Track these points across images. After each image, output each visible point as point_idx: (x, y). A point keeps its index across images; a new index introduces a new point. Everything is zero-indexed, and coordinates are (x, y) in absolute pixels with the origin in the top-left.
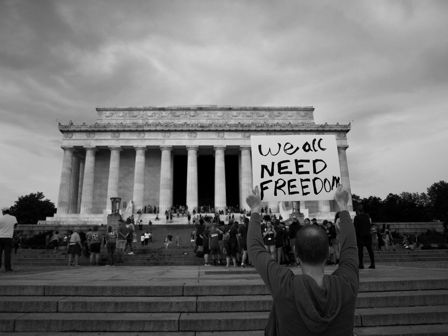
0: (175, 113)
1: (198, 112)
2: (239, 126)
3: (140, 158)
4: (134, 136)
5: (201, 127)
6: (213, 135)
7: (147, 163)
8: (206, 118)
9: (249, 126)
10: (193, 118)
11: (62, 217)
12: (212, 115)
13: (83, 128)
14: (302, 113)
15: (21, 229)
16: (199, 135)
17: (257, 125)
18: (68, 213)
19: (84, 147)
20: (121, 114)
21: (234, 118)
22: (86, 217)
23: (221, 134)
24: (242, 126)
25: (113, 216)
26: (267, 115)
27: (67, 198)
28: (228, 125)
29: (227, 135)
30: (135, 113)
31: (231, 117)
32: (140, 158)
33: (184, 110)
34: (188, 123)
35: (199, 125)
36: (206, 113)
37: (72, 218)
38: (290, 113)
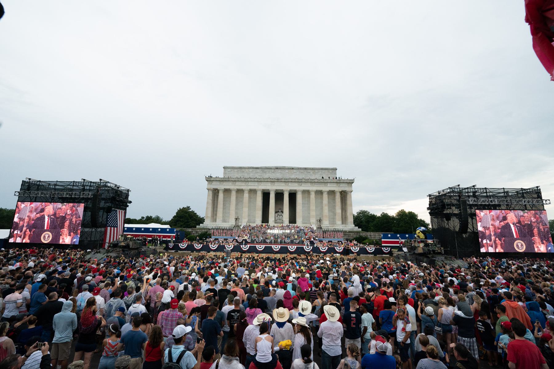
3: (246, 195)
4: (243, 184)
6: (283, 184)
7: (250, 198)
9: (301, 179)
11: (208, 224)
13: (218, 179)
14: (331, 171)
16: (276, 184)
20: (236, 170)
22: (220, 224)
23: (287, 183)
24: (298, 179)
26: (311, 172)
27: (210, 214)
29: (290, 184)
30: (243, 170)
32: (246, 195)
36: (280, 171)
38: (324, 171)
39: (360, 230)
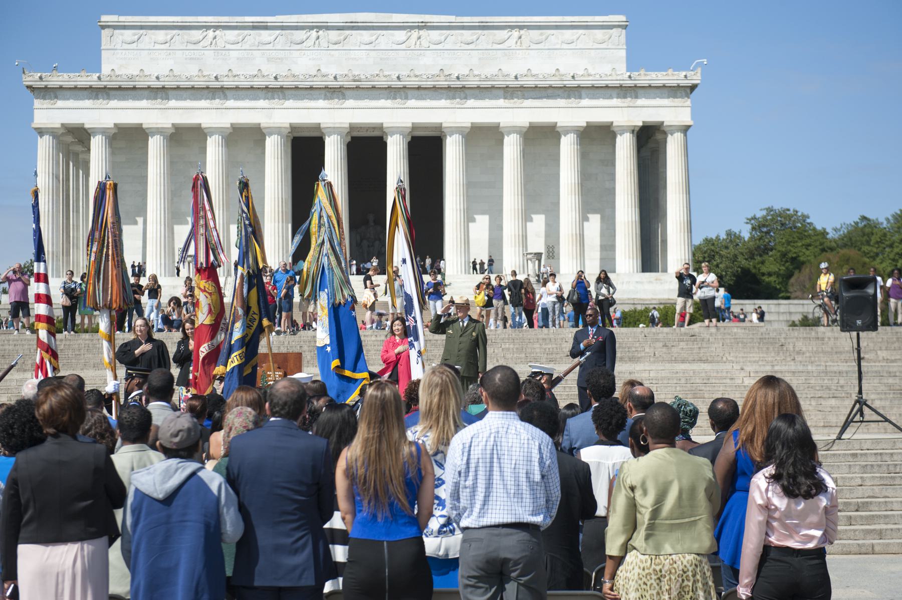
0: (293, 34)
1: (347, 32)
2: (442, 78)
8: (367, 47)
10: (336, 47)
17: (483, 77)
19: (86, 126)
21: (433, 47)
28: (416, 76)
33: (311, 28)
35: (351, 78)
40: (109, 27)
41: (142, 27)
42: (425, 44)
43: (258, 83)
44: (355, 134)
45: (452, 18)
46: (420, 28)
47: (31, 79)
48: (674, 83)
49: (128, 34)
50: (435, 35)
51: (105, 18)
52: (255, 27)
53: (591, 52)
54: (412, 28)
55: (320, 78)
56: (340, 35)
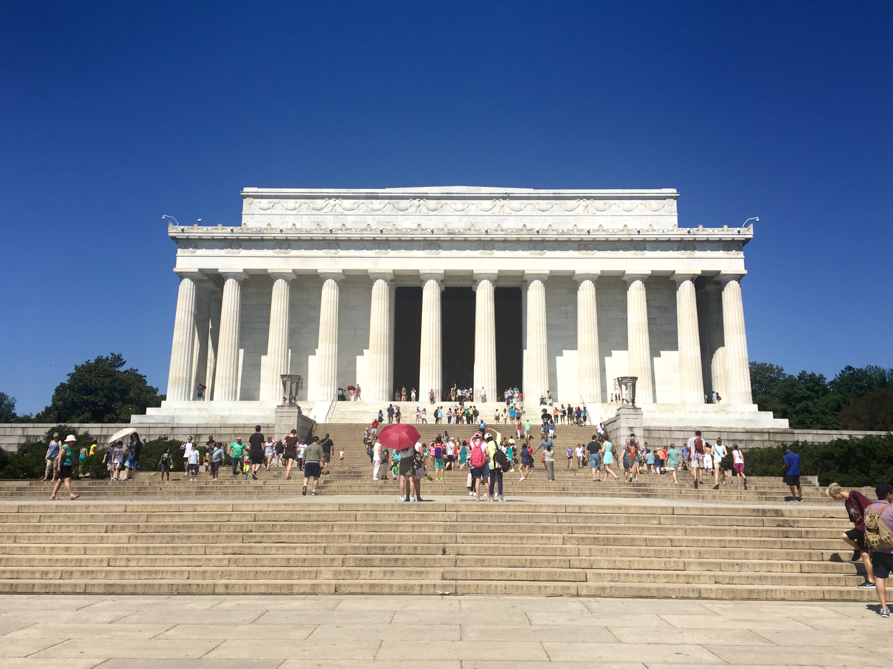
2: (525, 232)
5: (449, 234)
7: (344, 307)
8: (460, 213)
10: (434, 213)
12: (471, 207)
15: (104, 432)
18: (189, 399)
19: (220, 271)
21: (514, 213)
25: (286, 409)
31: (510, 211)
33: (415, 198)
34: (423, 226)
35: (446, 231)
37: (199, 409)
39: (784, 423)
40: (249, 196)
41: (276, 197)
42: (507, 210)
43: (367, 235)
44: (450, 284)
45: (531, 191)
46: (504, 198)
47: (174, 231)
48: (728, 237)
49: (265, 203)
50: (516, 204)
51: (246, 190)
52: (368, 197)
53: (652, 213)
54: (497, 198)
55: (419, 232)
56: (437, 204)
